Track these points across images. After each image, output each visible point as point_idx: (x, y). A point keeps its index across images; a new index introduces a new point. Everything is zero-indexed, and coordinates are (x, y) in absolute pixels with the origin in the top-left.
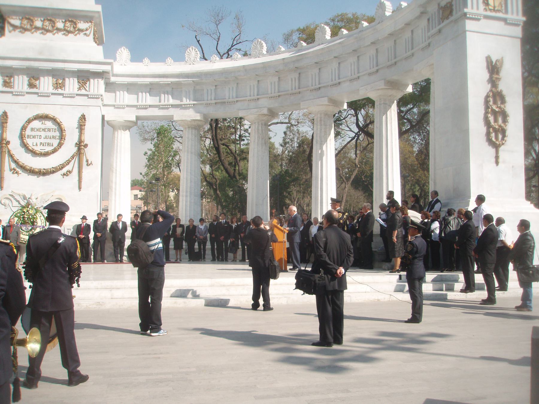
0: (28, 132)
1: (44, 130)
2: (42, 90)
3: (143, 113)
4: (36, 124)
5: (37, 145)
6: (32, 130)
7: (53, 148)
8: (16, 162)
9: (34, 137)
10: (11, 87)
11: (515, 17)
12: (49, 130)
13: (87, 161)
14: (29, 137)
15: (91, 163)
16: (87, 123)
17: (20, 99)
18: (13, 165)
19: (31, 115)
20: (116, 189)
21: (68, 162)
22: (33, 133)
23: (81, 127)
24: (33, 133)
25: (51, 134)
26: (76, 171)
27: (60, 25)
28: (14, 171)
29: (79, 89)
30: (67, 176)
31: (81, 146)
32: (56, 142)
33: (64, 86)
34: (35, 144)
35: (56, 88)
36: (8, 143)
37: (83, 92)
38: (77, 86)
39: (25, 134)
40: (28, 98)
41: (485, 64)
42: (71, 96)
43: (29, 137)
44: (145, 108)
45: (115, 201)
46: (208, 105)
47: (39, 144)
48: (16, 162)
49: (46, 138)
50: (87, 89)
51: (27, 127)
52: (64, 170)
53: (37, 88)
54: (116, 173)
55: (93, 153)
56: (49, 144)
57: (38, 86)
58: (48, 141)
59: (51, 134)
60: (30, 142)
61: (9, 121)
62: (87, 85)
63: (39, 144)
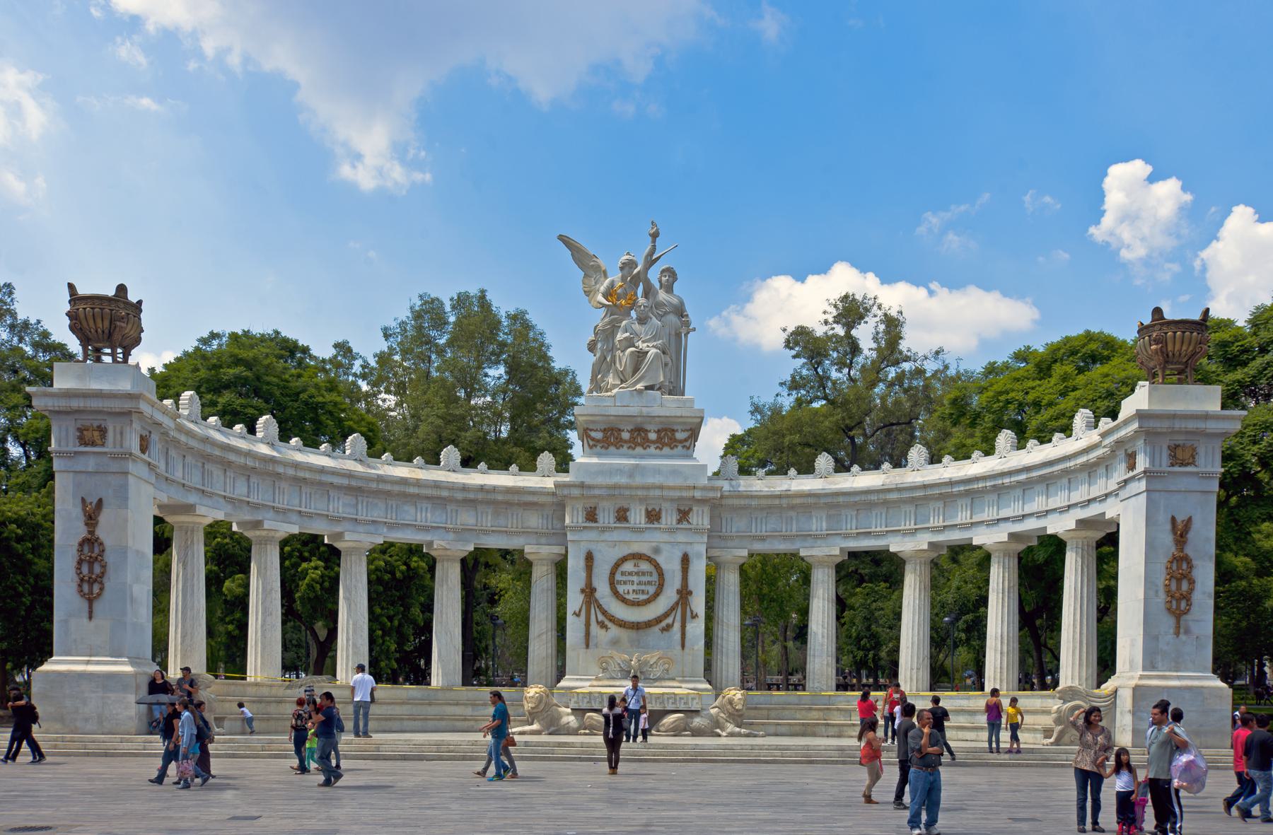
0: (618, 577)
1: (637, 574)
3: (759, 547)
4: (628, 567)
6: (623, 574)
9: (625, 583)
10: (596, 521)
11: (1209, 469)
12: (643, 574)
14: (619, 582)
17: (607, 536)
19: (621, 556)
22: (624, 578)
24: (624, 578)
25: (644, 579)
26: (677, 626)
27: (653, 436)
29: (679, 521)
31: (684, 593)
32: (652, 589)
35: (652, 522)
36: (593, 590)
37: (685, 525)
38: (675, 517)
40: (615, 536)
41: (1169, 527)
42: (671, 531)
43: (619, 582)
44: (762, 539)
46: (847, 536)
49: (640, 583)
56: (643, 592)
58: (643, 587)
59: (644, 579)
60: (621, 589)
61: (596, 563)
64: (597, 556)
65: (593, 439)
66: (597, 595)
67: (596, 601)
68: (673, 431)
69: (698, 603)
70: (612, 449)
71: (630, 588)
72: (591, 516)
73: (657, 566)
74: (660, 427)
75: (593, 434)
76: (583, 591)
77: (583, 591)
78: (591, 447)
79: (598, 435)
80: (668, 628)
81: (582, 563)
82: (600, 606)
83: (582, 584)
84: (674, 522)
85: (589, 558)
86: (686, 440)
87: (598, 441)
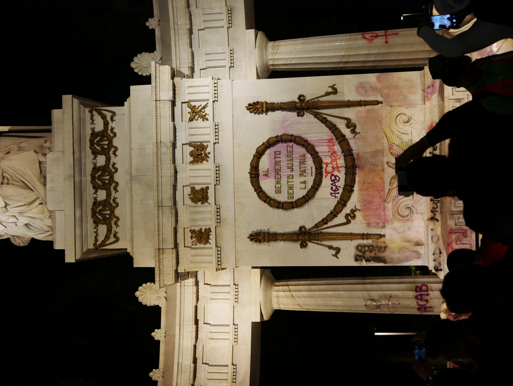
0: (283, 198)
1: (278, 172)
2: (211, 180)
4: (267, 185)
5: (304, 182)
6: (278, 191)
7: (309, 156)
8: (334, 214)
9: (291, 188)
10: (209, 230)
12: (277, 163)
13: (327, 94)
15: (333, 87)
16: (262, 100)
17: (227, 214)
18: (341, 218)
20: (378, 54)
21: (333, 128)
22: (285, 189)
23: (271, 107)
24: (285, 189)
27: (101, 160)
28: (351, 217)
29: (204, 118)
30: (355, 127)
32: (299, 150)
33: (201, 143)
34: (303, 186)
37: (208, 111)
38: (199, 122)
39: (286, 203)
45: (399, 53)
47: (303, 179)
48: (334, 214)
50: (203, 104)
51: (274, 200)
52: (346, 132)
53: (207, 188)
54: (350, 56)
55: (313, 87)
57: (204, 186)
58: (296, 163)
60: (299, 193)
62: (197, 104)
63: (303, 179)
64: (256, 228)
65: (107, 237)
66: (309, 225)
67: (316, 226)
68: (94, 135)
69: (313, 87)
70: (117, 212)
71: (297, 180)
72: (202, 236)
73: (269, 144)
74: (89, 151)
75: (101, 238)
76: (303, 245)
77: (303, 245)
78: (117, 240)
79: (103, 229)
80: (350, 124)
81: (264, 247)
82: (325, 221)
83: (297, 245)
84: (206, 123)
85: (258, 237)
86: (104, 117)
87: (109, 230)
